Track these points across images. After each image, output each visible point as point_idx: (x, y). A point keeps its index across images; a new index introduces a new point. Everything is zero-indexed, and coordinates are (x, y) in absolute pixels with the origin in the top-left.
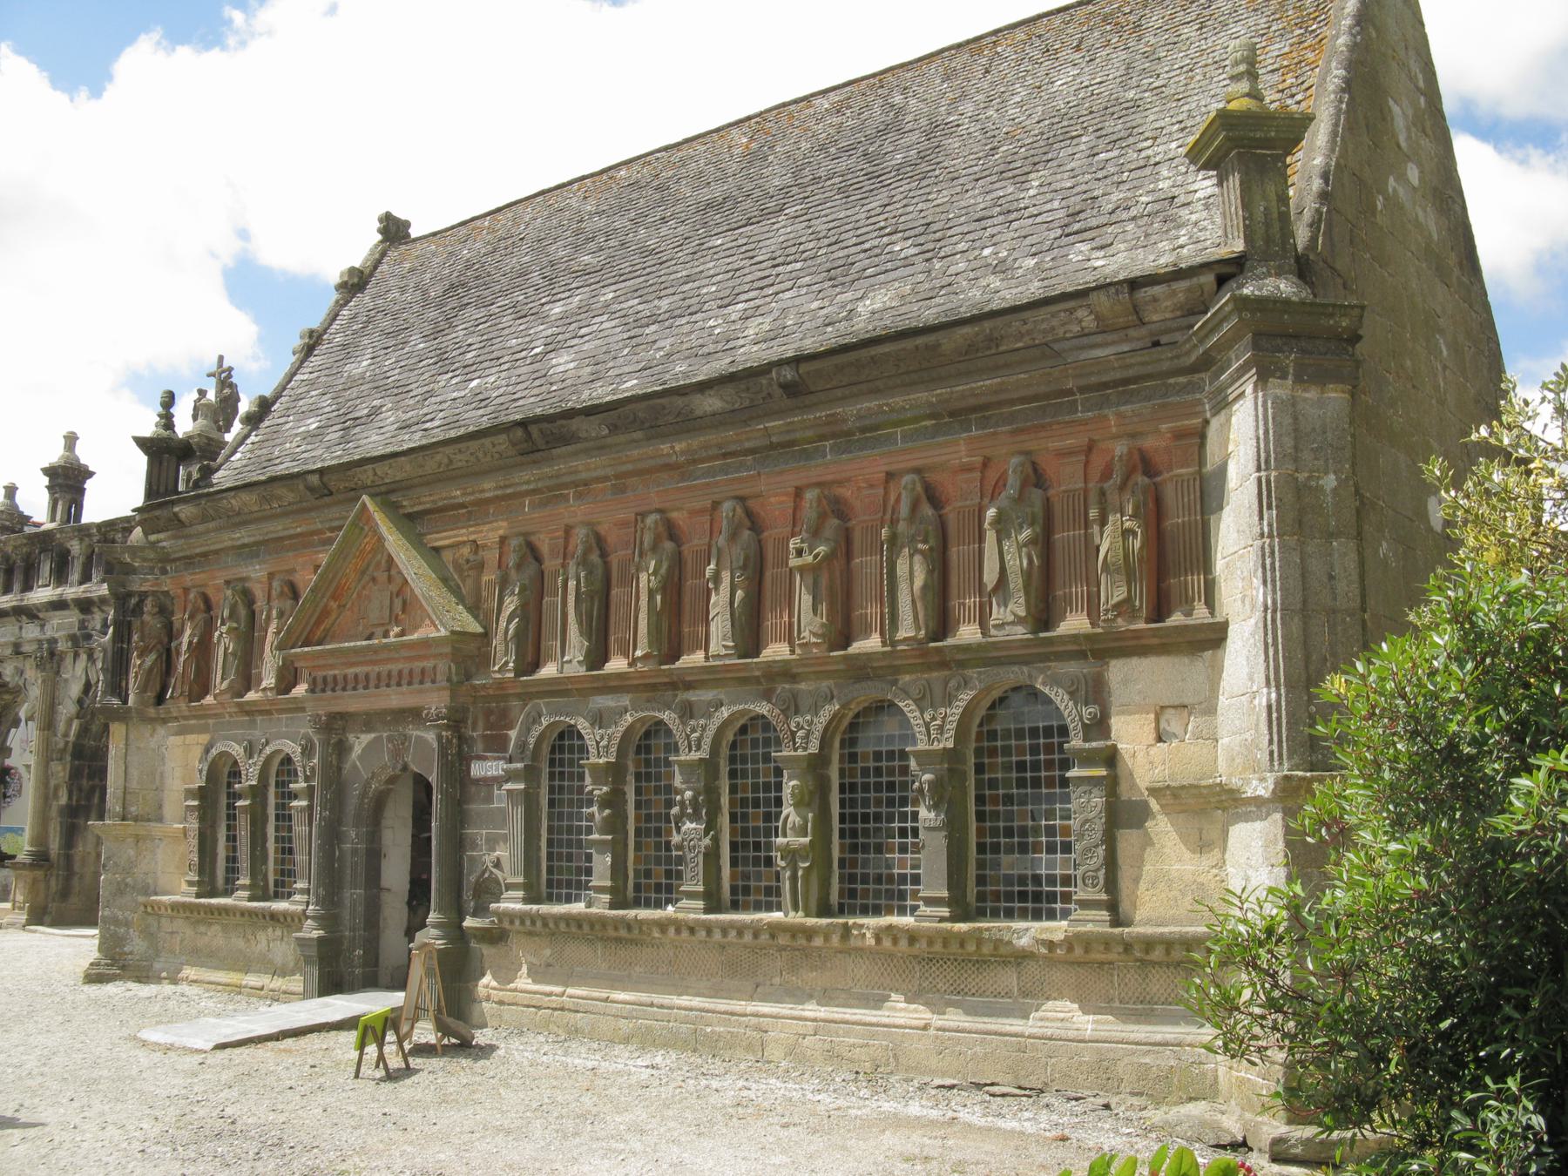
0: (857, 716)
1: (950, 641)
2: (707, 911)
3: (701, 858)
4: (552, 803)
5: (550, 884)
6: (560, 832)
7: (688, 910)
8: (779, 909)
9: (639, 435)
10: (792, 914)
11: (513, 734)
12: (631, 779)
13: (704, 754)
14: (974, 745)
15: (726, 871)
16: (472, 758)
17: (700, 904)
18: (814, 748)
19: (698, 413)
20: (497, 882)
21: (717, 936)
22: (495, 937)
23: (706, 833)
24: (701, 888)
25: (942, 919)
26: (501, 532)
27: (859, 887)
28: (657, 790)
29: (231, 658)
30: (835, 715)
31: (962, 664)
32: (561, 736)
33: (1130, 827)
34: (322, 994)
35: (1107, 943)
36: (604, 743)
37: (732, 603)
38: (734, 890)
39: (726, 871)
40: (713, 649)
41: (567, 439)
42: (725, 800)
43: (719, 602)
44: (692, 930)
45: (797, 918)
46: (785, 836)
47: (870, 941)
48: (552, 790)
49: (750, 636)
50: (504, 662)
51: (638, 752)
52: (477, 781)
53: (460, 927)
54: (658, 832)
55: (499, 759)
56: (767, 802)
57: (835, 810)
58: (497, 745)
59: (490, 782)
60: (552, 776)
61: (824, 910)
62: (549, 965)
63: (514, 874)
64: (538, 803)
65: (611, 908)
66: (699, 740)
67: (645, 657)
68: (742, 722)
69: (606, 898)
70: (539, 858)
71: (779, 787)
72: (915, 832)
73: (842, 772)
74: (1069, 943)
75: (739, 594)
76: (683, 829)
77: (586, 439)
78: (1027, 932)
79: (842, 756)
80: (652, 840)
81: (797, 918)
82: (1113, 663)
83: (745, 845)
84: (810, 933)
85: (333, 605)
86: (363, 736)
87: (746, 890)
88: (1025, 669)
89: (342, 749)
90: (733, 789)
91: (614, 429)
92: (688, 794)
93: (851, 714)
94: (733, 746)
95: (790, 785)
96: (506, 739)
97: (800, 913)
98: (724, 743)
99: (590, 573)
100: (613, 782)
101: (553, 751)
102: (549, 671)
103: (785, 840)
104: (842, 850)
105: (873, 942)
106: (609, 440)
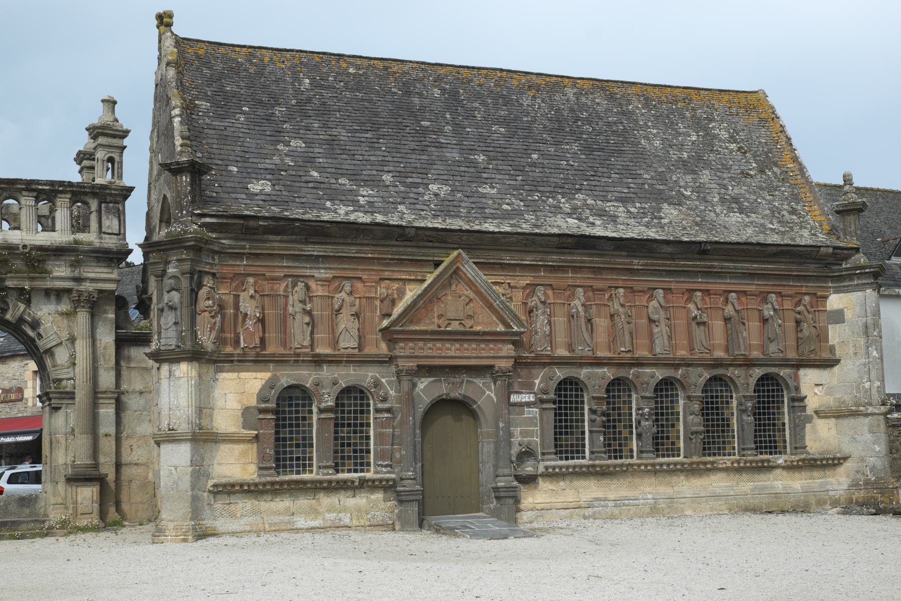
9: (624, 253)
11: (537, 382)
29: (305, 326)
40: (658, 350)
41: (593, 247)
52: (515, 404)
58: (528, 387)
59: (521, 405)
74: (798, 461)
86: (423, 380)
91: (617, 248)
92: (647, 410)
96: (533, 384)
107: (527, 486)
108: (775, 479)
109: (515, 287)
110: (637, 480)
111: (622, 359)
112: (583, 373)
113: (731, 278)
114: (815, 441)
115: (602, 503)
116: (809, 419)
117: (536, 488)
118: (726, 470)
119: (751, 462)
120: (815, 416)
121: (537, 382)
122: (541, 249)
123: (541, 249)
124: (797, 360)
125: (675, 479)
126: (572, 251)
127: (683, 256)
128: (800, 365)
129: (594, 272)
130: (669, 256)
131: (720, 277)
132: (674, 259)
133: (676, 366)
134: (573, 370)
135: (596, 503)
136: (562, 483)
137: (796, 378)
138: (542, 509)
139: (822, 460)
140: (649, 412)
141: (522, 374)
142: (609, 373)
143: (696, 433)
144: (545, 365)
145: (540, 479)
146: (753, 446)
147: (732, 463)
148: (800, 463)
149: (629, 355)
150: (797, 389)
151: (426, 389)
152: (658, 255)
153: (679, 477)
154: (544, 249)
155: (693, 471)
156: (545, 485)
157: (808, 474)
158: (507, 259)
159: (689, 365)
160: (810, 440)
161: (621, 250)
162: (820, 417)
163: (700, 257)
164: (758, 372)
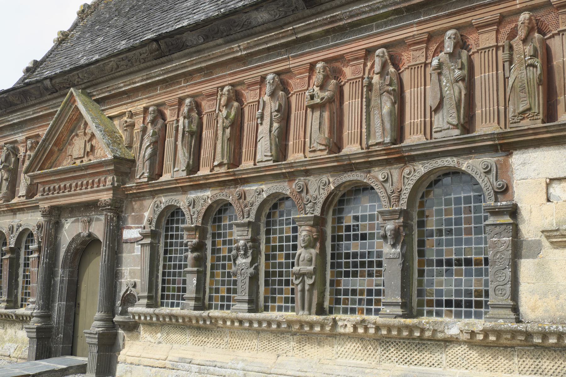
0: (344, 195)
1: (403, 145)
2: (250, 311)
3: (247, 280)
4: (166, 252)
5: (163, 297)
6: (170, 268)
7: (240, 310)
8: (293, 309)
9: (220, 41)
10: (301, 313)
11: (146, 214)
12: (209, 236)
13: (252, 219)
14: (417, 210)
15: (262, 289)
16: (124, 228)
17: (246, 306)
18: (318, 212)
19: (254, 23)
20: (134, 296)
21: (256, 325)
22: (132, 327)
23: (252, 263)
24: (247, 298)
25: (397, 316)
26: (144, 105)
27: (342, 297)
28: (224, 243)
30: (331, 193)
31: (413, 159)
32: (173, 215)
33: (528, 257)
34: (37, 359)
35: (514, 333)
36: (195, 216)
37: (270, 131)
38: (266, 299)
39: (262, 289)
40: (258, 158)
42: (263, 247)
43: (264, 129)
44: (241, 322)
45: (304, 316)
46: (298, 265)
47: (349, 329)
48: (166, 244)
49: (281, 150)
50: (142, 172)
51: (214, 222)
53: (112, 321)
54: (224, 267)
55: (138, 228)
56: (288, 247)
57: (329, 251)
60: (166, 237)
61: (321, 311)
62: (160, 343)
63: (143, 291)
64: (158, 253)
65: (194, 310)
66: (249, 211)
67: (221, 165)
68: (274, 201)
69: (192, 303)
70: (157, 282)
71: (295, 238)
72: (380, 264)
73: (333, 228)
74: (486, 332)
75: (276, 125)
76: (237, 262)
77: (191, 47)
78: (454, 326)
79: (333, 220)
80: (220, 271)
81: (304, 316)
82: (515, 152)
83: (274, 274)
84: (311, 325)
85: (56, 149)
86: (69, 220)
87: (274, 300)
88: (455, 159)
89: (58, 226)
90: (268, 241)
91: (207, 38)
92: (242, 243)
93: (340, 194)
94: (269, 216)
95: (303, 233)
97: (306, 312)
98: (264, 214)
99: (190, 123)
100: (199, 238)
101: (167, 224)
102: (166, 177)
103: (298, 268)
104: (332, 276)
105: (352, 330)
106: (203, 46)
107: (130, 334)
108: (452, 365)
109: (136, 114)
110: (236, 341)
111: (217, 176)
112: (182, 201)
113: (378, 27)
114: (545, 295)
115: (187, 366)
116: (536, 250)
117: (137, 338)
118: (353, 337)
119: (389, 329)
120: (546, 243)
121: (146, 214)
122: (142, 66)
123: (142, 66)
124: (492, 137)
125: (283, 345)
126: (170, 57)
127: (290, 19)
128: (506, 145)
129: (205, 75)
130: (271, 25)
131: (360, 31)
132: (281, 27)
133: (290, 176)
134: (173, 197)
135: (180, 365)
136: (159, 335)
137: (503, 170)
138: (131, 364)
139: (545, 335)
140: (245, 245)
141: (135, 207)
142: (207, 196)
143: (303, 275)
144: (154, 194)
145: (141, 328)
146: (399, 300)
147: (355, 328)
148: (492, 338)
149: (223, 170)
150: (505, 190)
151: (71, 230)
152: (259, 29)
153: (289, 343)
154: (145, 65)
155: (304, 334)
156: (145, 335)
157: (529, 362)
158: (122, 85)
159: (307, 173)
160: (532, 292)
161: (213, 39)
162: (556, 245)
163: (308, 12)
164: (422, 168)
